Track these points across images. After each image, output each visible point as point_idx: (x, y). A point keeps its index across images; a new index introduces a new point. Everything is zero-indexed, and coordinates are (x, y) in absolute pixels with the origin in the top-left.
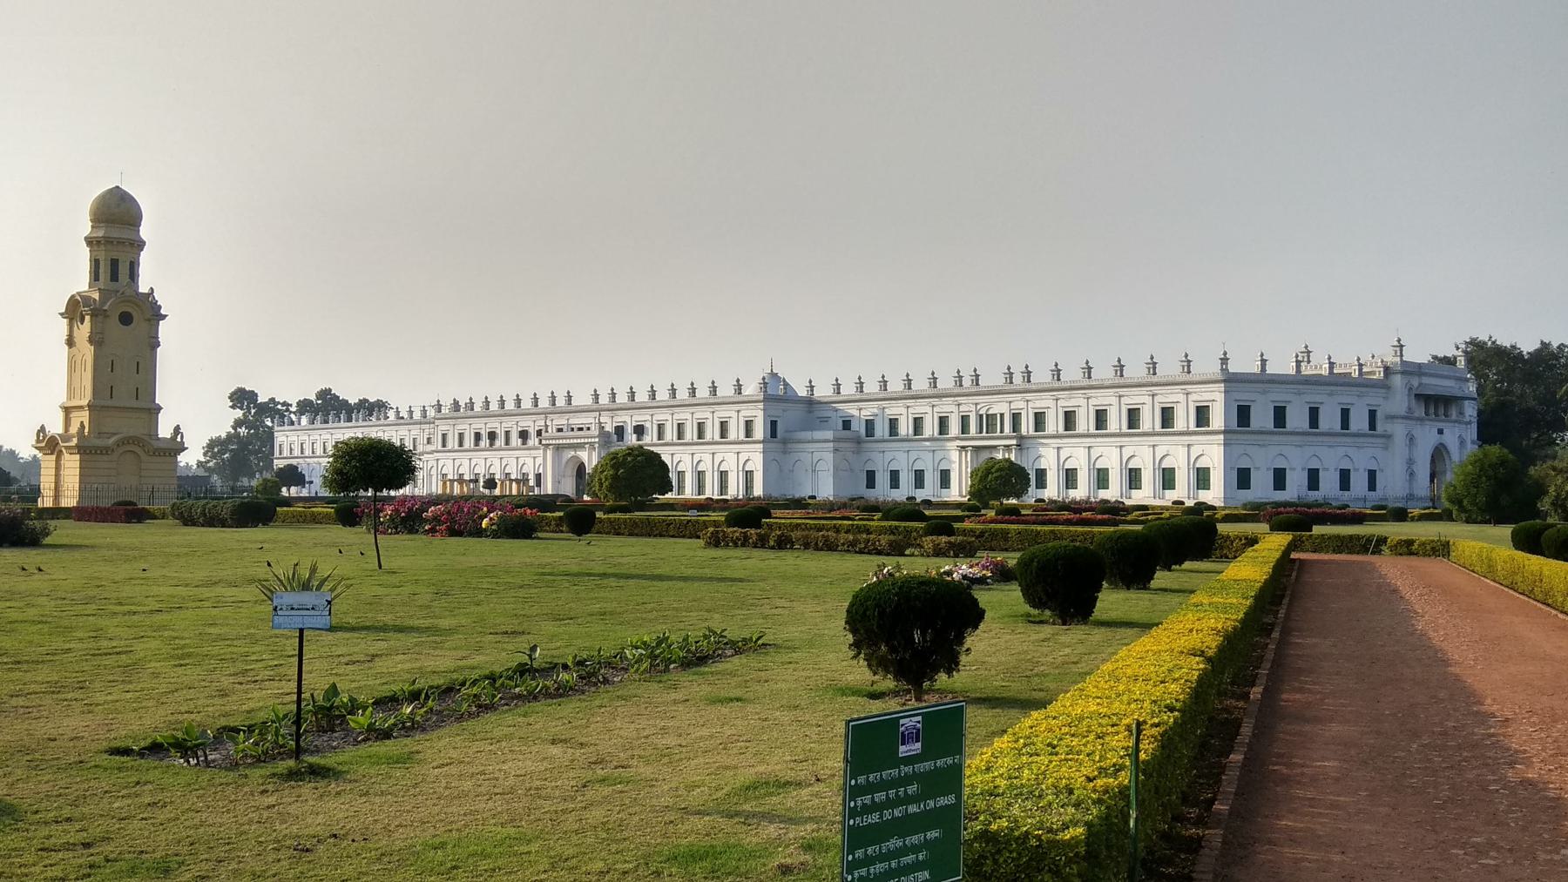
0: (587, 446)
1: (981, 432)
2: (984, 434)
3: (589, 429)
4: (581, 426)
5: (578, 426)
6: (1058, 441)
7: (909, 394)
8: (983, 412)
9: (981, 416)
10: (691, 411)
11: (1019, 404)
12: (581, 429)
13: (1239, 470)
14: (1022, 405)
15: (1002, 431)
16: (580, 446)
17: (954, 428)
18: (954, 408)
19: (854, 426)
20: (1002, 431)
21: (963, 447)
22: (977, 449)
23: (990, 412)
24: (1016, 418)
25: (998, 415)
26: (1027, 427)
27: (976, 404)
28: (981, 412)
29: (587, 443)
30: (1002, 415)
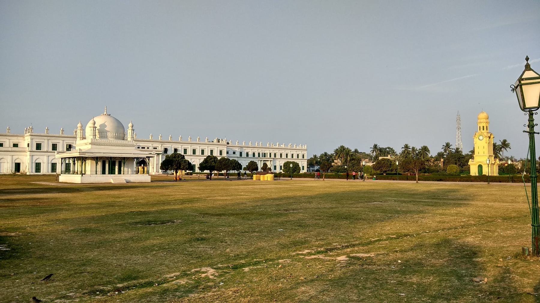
1: (262, 157)
2: (263, 157)
3: (148, 148)
6: (280, 160)
8: (263, 152)
9: (262, 153)
10: (217, 147)
11: (271, 151)
12: (142, 148)
14: (272, 151)
15: (267, 157)
18: (257, 151)
20: (267, 157)
23: (264, 152)
27: (262, 150)
30: (267, 153)
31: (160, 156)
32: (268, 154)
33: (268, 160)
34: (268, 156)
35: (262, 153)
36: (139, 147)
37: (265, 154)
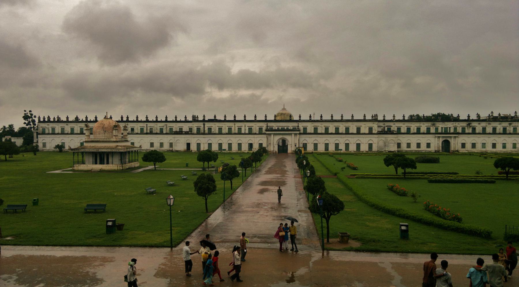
0: (292, 134)
4: (288, 127)
5: (287, 127)
7: (215, 120)
13: (472, 144)
16: (291, 134)
17: (433, 130)
19: (392, 129)
21: (439, 137)
22: (443, 137)
24: (455, 129)
25: (448, 128)
26: (460, 130)
28: (442, 127)
29: (293, 133)
30: (450, 128)
31: (298, 136)
32: (451, 128)
33: (451, 137)
34: (452, 131)
35: (442, 128)
36: (278, 127)
37: (446, 128)
